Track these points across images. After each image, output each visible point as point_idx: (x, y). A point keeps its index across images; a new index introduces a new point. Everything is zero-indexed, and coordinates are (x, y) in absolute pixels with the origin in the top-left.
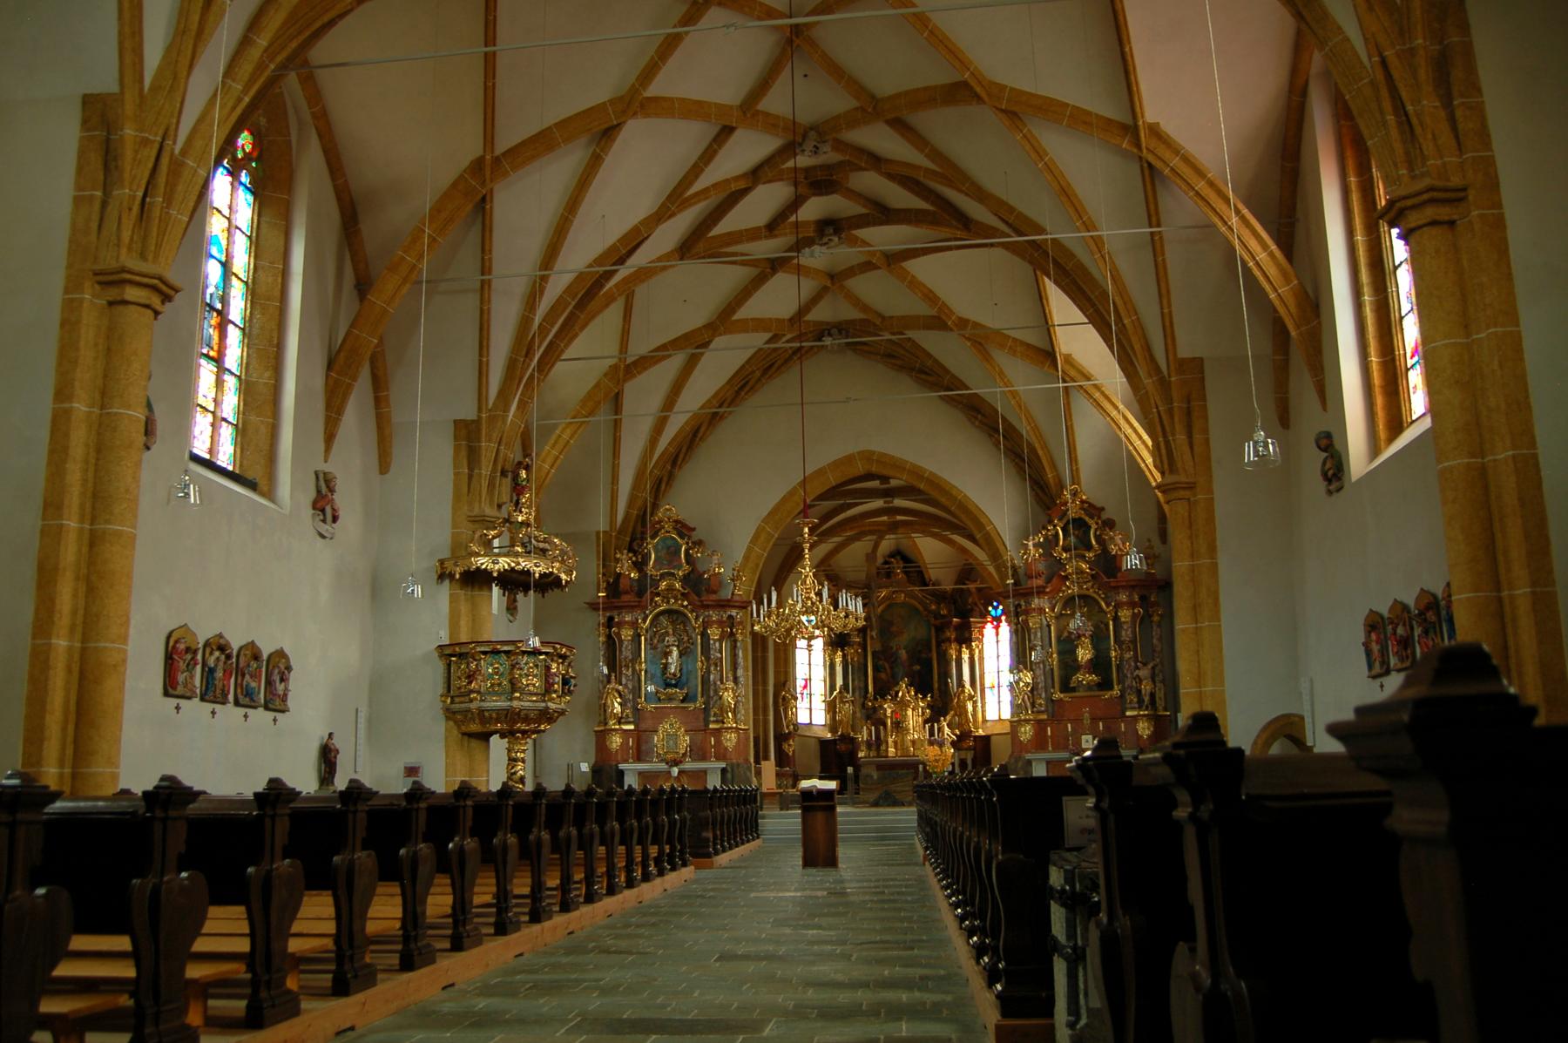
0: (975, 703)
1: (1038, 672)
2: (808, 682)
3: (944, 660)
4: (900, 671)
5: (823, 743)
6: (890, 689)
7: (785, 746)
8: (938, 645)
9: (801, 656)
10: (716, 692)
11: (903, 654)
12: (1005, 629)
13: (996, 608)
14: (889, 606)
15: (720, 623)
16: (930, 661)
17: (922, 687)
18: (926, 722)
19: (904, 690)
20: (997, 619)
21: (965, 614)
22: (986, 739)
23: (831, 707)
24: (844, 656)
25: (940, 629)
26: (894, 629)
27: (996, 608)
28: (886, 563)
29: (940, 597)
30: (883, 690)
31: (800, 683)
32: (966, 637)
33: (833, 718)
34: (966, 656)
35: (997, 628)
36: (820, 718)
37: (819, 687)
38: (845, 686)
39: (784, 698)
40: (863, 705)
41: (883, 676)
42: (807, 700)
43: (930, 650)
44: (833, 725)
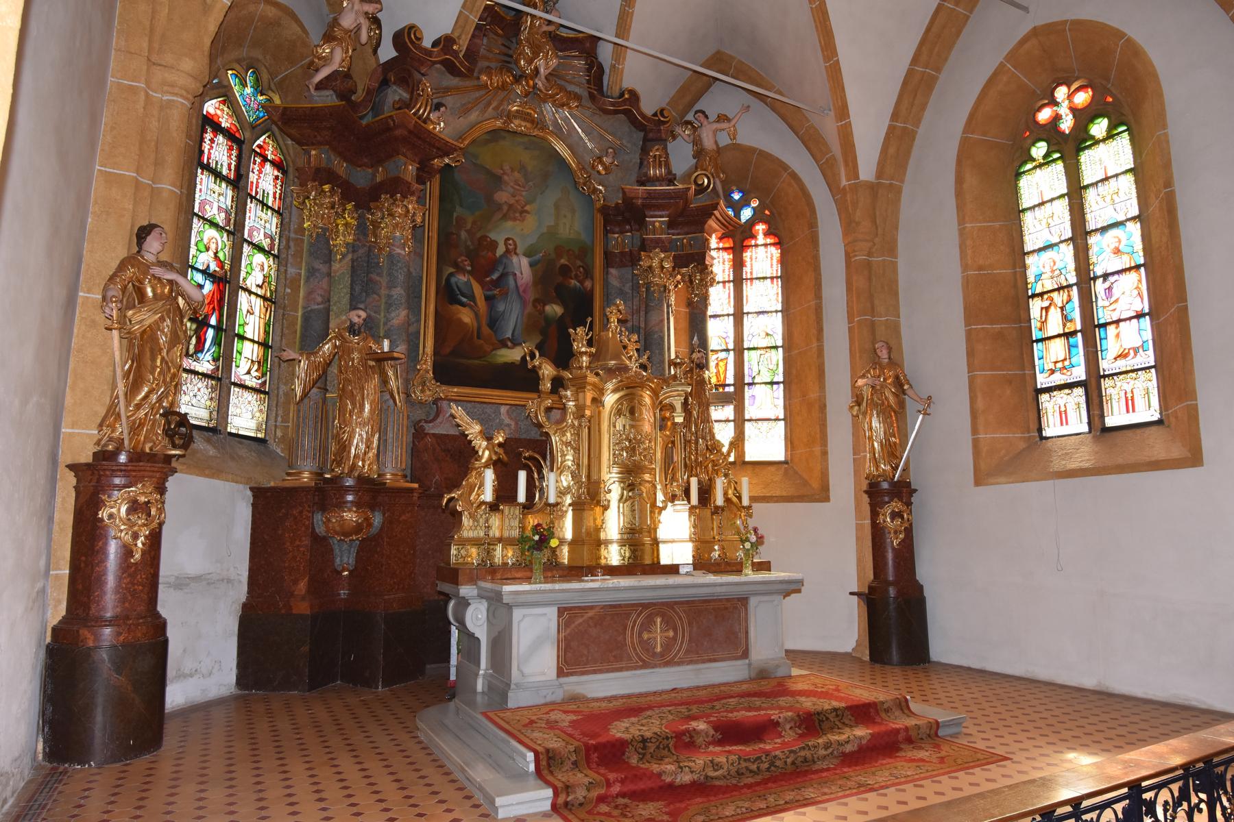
11: (522, 267)
26: (502, 196)
41: (466, 316)
43: (588, 274)
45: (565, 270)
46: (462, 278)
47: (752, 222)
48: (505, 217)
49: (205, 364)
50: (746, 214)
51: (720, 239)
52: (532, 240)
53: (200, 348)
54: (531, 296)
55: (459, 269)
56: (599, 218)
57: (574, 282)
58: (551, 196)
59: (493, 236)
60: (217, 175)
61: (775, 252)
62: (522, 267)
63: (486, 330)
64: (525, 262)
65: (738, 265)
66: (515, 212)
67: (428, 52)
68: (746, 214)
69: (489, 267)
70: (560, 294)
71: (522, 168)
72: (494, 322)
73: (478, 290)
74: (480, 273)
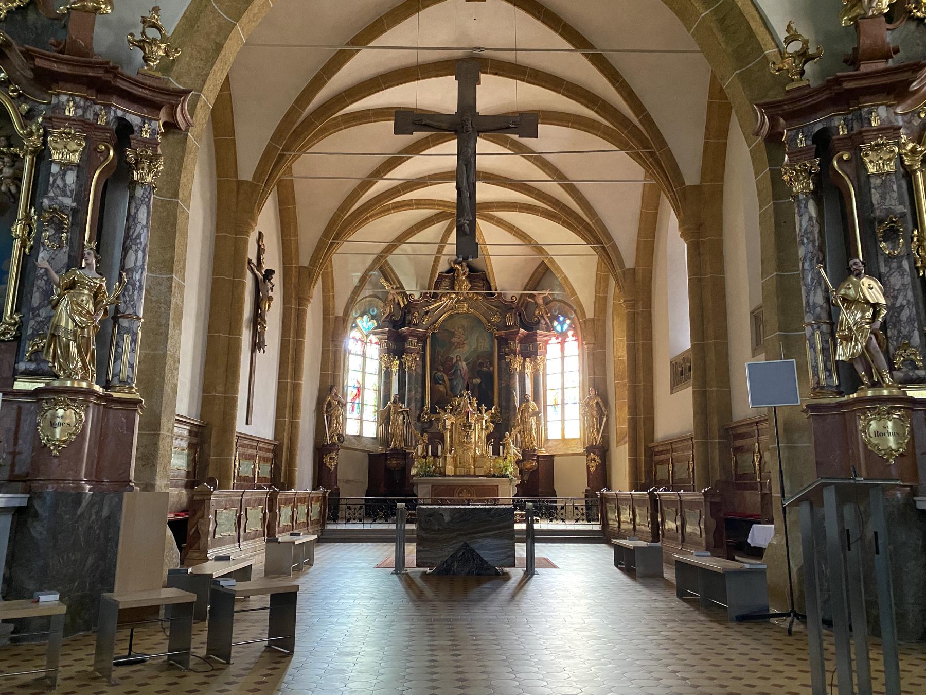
0: (538, 420)
1: (896, 281)
2: (360, 391)
3: (507, 372)
4: (460, 384)
5: (373, 458)
6: (449, 402)
7: (327, 460)
8: (501, 357)
9: (353, 363)
10: (48, 293)
11: (463, 366)
12: (572, 346)
13: (562, 324)
14: (451, 316)
15: (86, 126)
16: (491, 375)
17: (485, 399)
18: (488, 438)
19: (467, 402)
20: (564, 335)
21: (531, 326)
22: (550, 459)
23: (385, 419)
24: (401, 365)
25: (503, 341)
26: (455, 340)
27: (562, 324)
28: (451, 270)
29: (506, 307)
30: (441, 402)
31: (351, 393)
32: (530, 351)
33: (387, 430)
34: (529, 371)
35: (562, 343)
36: (371, 430)
37: (371, 398)
38: (401, 397)
39: (329, 404)
40: (419, 418)
41: (442, 388)
42: (356, 411)
43: (492, 364)
44: (385, 437)
45: (481, 364)
46: (440, 374)
47: (567, 330)
48: (456, 348)
49: (356, 414)
50: (566, 327)
51: (557, 338)
52: (466, 355)
53: (353, 410)
54: (467, 377)
55: (439, 370)
56: (496, 342)
57: (485, 369)
58: (475, 336)
59: (451, 356)
60: (356, 355)
61: (576, 343)
62: (463, 366)
63: (449, 392)
64: (464, 363)
65: (562, 349)
66: (460, 345)
67: (418, 301)
68: (566, 327)
69: (450, 368)
70: (480, 374)
71: (463, 327)
72: (452, 388)
73: (446, 378)
74: (446, 371)
